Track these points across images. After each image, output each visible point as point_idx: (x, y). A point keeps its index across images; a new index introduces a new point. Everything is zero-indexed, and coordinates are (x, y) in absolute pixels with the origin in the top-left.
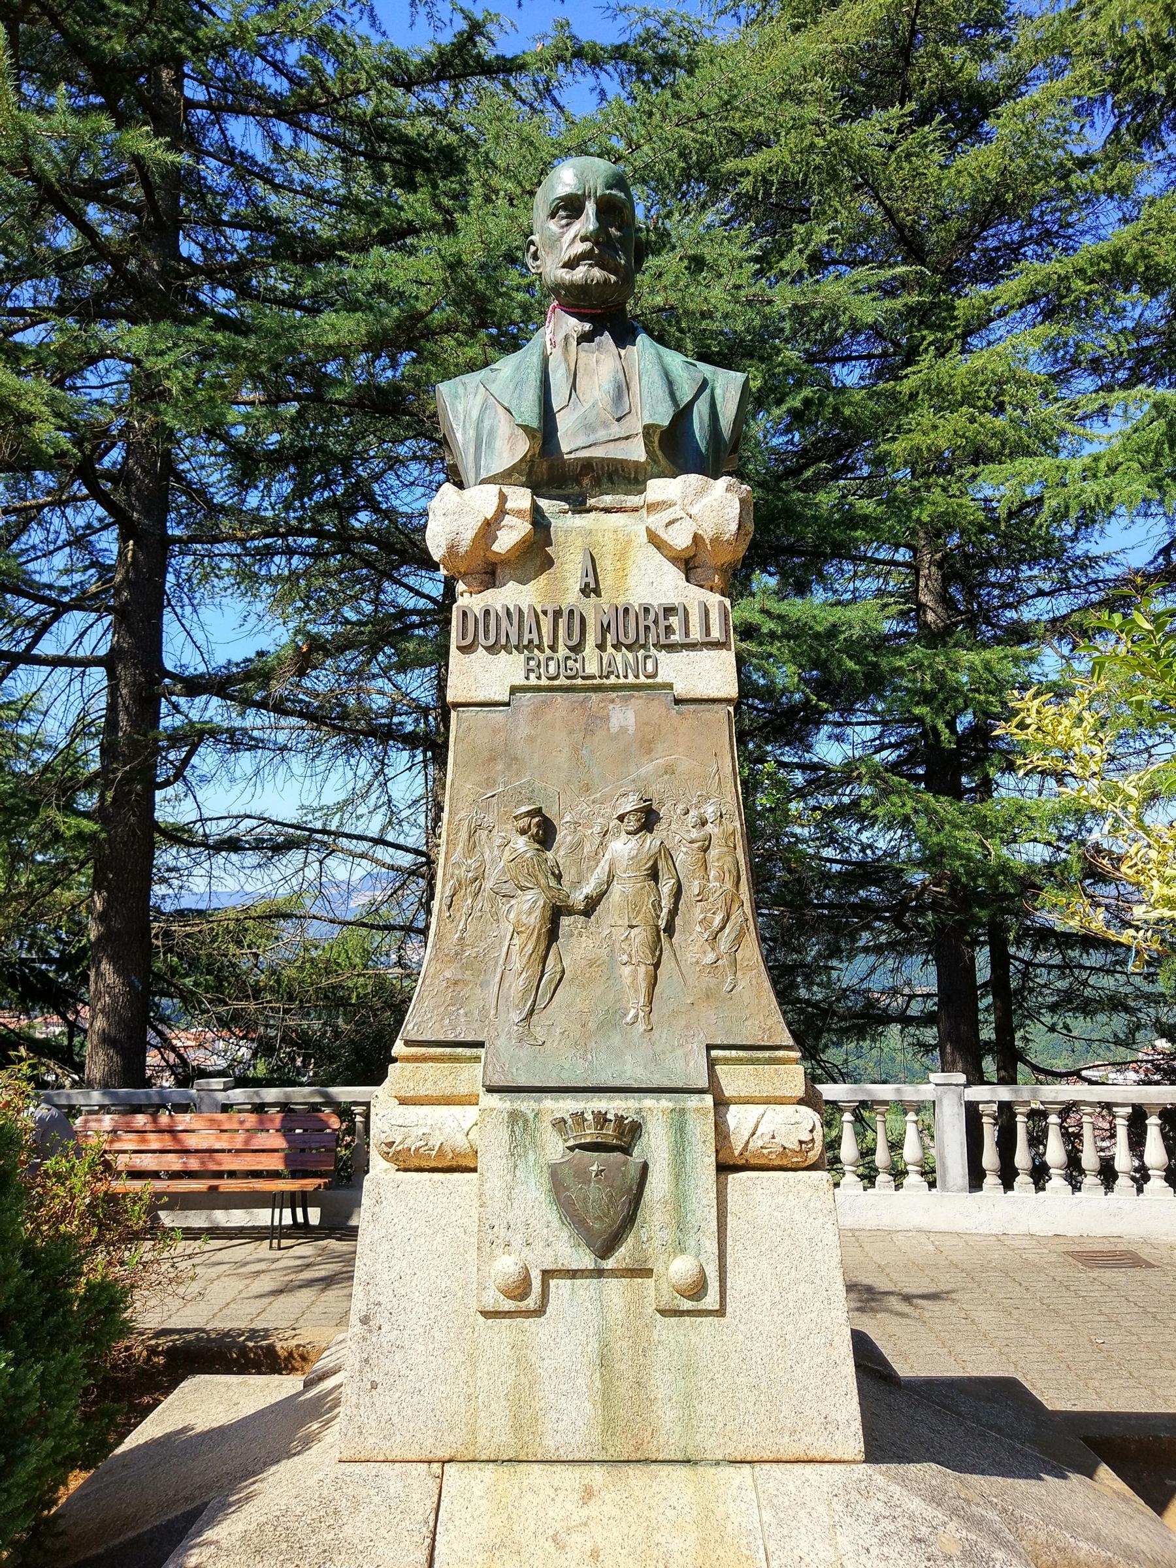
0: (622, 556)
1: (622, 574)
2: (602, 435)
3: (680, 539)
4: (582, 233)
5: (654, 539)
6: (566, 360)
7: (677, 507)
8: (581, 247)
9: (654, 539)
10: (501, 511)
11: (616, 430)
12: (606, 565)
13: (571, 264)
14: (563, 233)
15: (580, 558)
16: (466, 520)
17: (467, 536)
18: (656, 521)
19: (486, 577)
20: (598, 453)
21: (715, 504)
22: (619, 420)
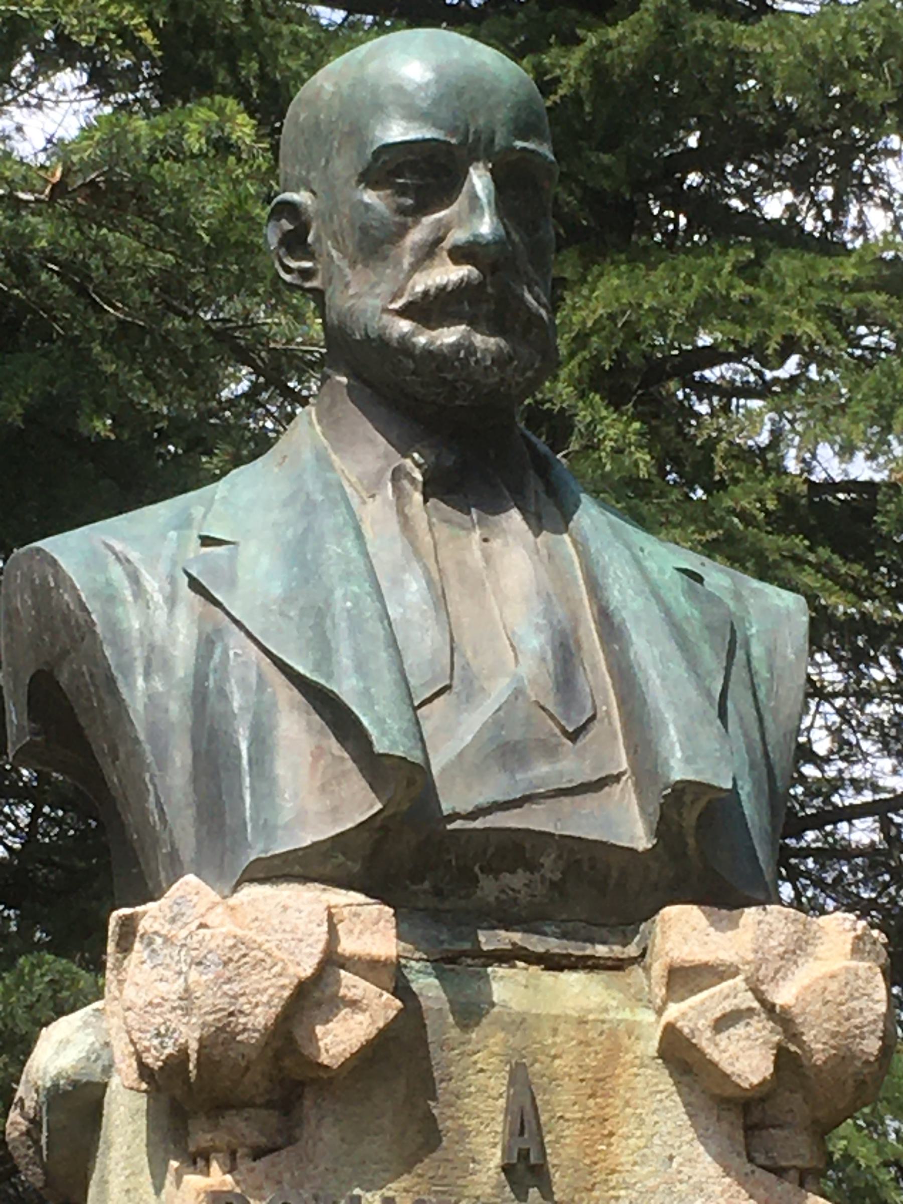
0: (598, 1084)
1: (601, 1126)
2: (542, 772)
3: (746, 1059)
4: (458, 236)
5: (680, 1056)
6: (417, 553)
7: (739, 981)
8: (448, 274)
9: (680, 1056)
10: (332, 961)
11: (572, 766)
12: (561, 1104)
13: (429, 309)
14: (403, 231)
15: (498, 1084)
16: (255, 980)
17: (260, 1017)
18: (692, 1012)
19: (272, 1118)
20: (535, 819)
21: (834, 986)
22: (574, 736)
